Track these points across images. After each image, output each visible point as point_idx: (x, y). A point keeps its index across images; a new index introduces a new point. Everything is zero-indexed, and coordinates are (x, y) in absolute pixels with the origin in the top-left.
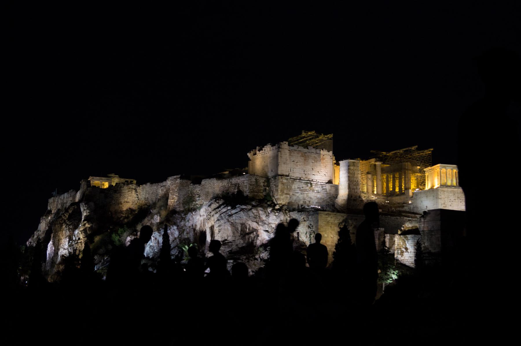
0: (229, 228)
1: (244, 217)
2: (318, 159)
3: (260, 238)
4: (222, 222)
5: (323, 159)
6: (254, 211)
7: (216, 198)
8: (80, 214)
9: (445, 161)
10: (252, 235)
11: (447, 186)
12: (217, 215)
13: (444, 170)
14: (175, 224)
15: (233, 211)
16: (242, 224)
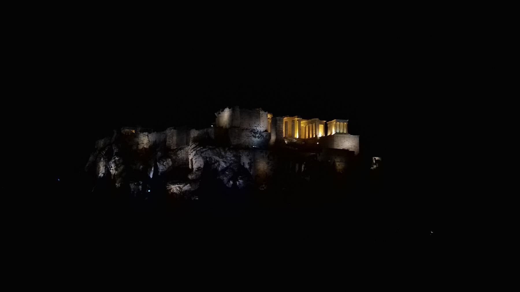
0: (202, 160)
1: (211, 153)
2: (258, 117)
3: (220, 166)
4: (197, 156)
5: (262, 116)
6: (217, 150)
7: (195, 140)
8: (113, 151)
9: (339, 117)
10: (216, 165)
11: (340, 133)
12: (194, 152)
13: (338, 123)
14: (171, 158)
15: (204, 150)
16: (210, 158)
